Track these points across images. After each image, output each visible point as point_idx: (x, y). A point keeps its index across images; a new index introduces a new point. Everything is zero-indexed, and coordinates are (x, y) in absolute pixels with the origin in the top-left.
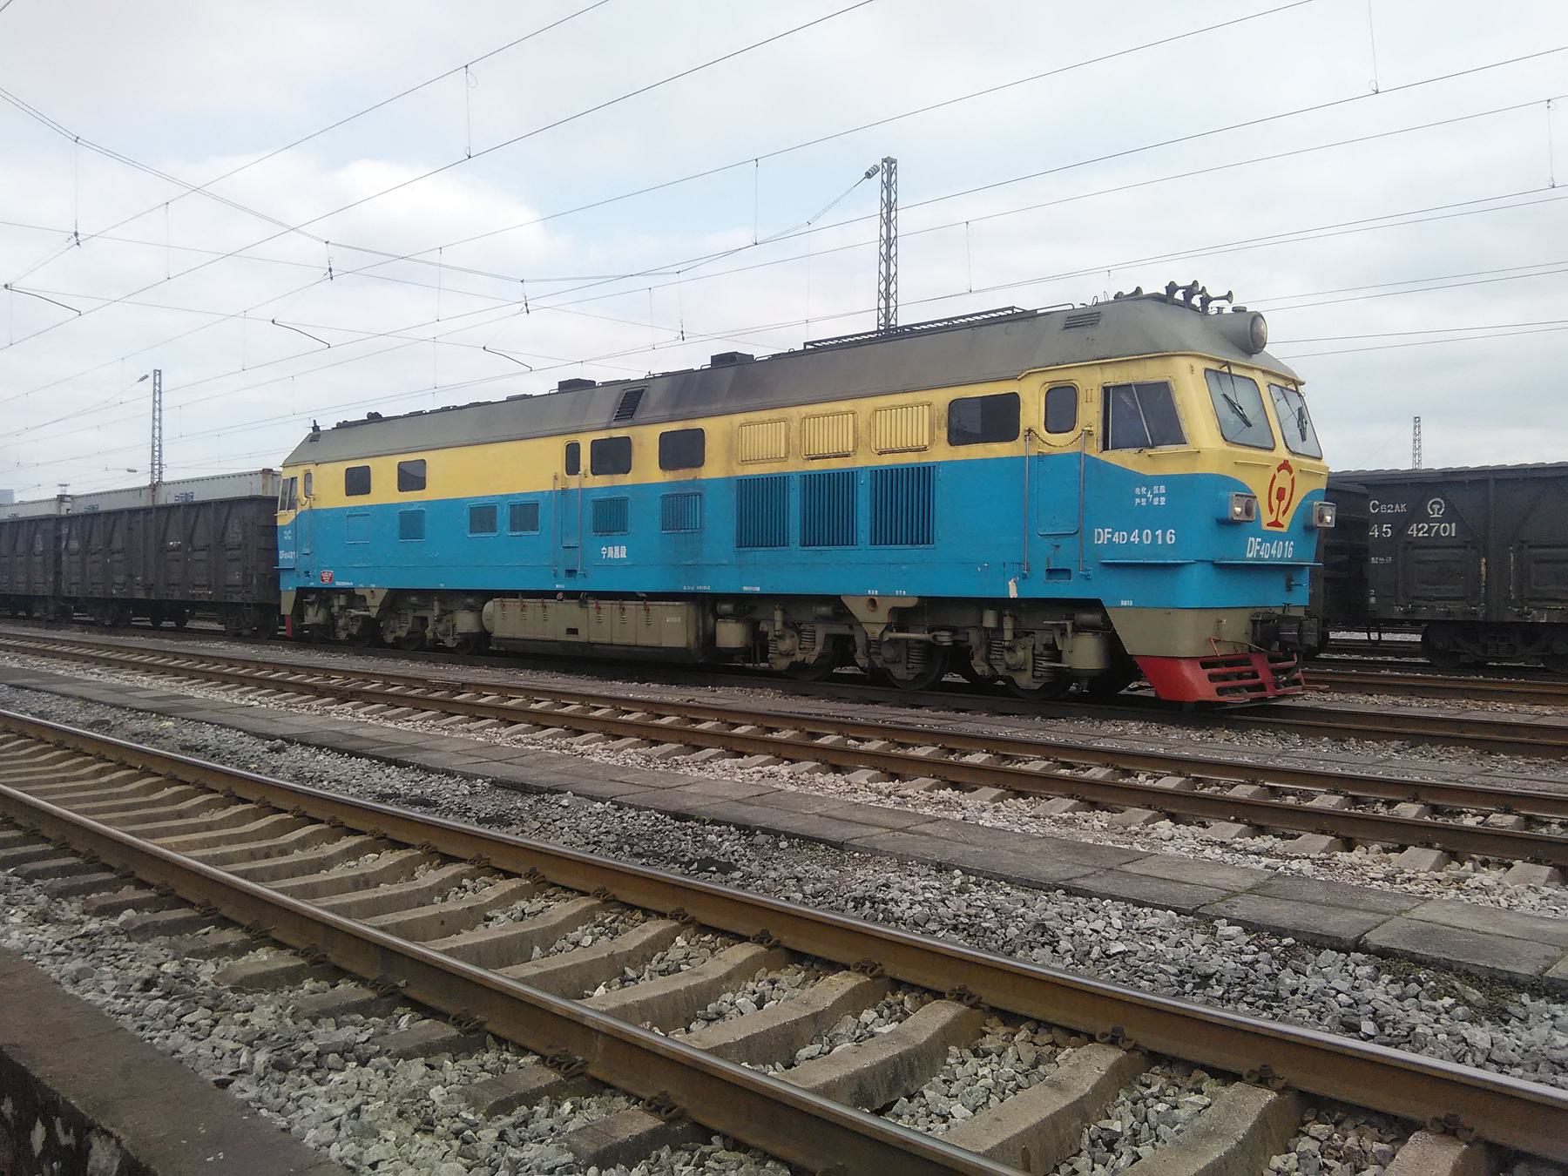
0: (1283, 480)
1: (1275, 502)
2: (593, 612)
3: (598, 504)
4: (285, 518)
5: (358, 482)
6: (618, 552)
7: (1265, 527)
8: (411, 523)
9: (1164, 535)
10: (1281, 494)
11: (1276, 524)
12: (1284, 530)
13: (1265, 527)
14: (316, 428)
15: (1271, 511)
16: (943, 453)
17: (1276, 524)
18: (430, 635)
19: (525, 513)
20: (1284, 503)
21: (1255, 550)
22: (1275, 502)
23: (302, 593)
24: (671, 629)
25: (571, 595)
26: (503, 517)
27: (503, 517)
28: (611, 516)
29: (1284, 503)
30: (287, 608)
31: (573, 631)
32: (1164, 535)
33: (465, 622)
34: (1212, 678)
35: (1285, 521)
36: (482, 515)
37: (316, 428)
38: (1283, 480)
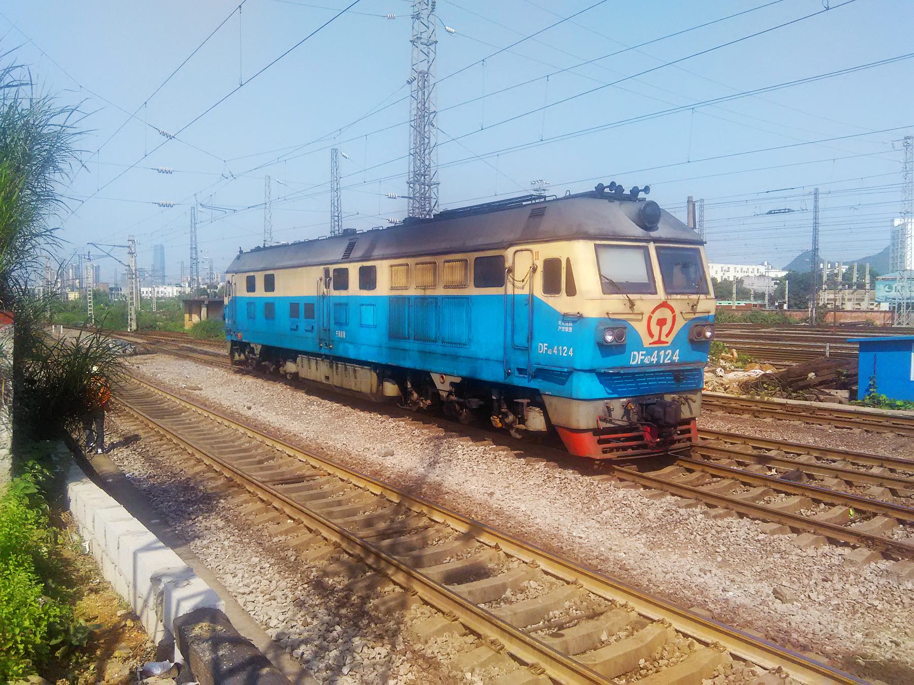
1: (655, 329)
8: (269, 308)
9: (568, 350)
10: (661, 322)
11: (659, 341)
14: (241, 252)
15: (652, 335)
17: (659, 341)
20: (666, 329)
21: (637, 358)
22: (655, 329)
25: (327, 357)
26: (302, 309)
27: (302, 309)
29: (666, 329)
32: (568, 350)
34: (600, 442)
36: (294, 307)
37: (241, 252)
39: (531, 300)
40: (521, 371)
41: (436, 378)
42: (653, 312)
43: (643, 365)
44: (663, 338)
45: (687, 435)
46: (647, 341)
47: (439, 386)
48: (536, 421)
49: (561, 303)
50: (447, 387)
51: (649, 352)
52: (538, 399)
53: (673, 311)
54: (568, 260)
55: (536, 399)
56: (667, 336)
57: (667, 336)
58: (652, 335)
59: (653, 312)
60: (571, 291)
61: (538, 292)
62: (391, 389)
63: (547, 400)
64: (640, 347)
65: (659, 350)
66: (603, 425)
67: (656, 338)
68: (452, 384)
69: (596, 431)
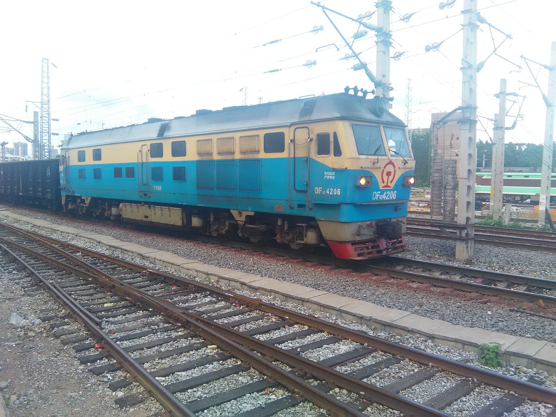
0: (390, 168)
1: (385, 178)
2: (153, 210)
3: (153, 169)
4: (61, 168)
5: (81, 157)
6: (159, 188)
7: (381, 188)
8: (97, 173)
10: (389, 174)
12: (392, 188)
13: (381, 188)
15: (383, 182)
16: (262, 155)
17: (387, 186)
18: (106, 215)
19: (130, 171)
21: (377, 196)
22: (385, 178)
23: (67, 197)
24: (175, 218)
25: (146, 203)
28: (157, 173)
29: (391, 178)
30: (63, 202)
31: (146, 217)
33: (114, 211)
35: (392, 185)
36: (118, 171)
38: (390, 168)
39: (307, 160)
40: (300, 206)
41: (234, 213)
42: (384, 168)
43: (379, 201)
44: (389, 184)
45: (401, 244)
46: (381, 185)
47: (237, 218)
48: (311, 237)
49: (329, 160)
50: (243, 218)
51: (382, 193)
52: (313, 223)
53: (395, 168)
54: (335, 134)
55: (311, 223)
56: (391, 182)
57: (391, 182)
58: (383, 182)
59: (384, 168)
60: (338, 152)
61: (314, 156)
62: (196, 222)
63: (320, 224)
64: (378, 189)
65: (387, 190)
66: (358, 238)
67: (385, 184)
68: (247, 216)
69: (354, 243)
